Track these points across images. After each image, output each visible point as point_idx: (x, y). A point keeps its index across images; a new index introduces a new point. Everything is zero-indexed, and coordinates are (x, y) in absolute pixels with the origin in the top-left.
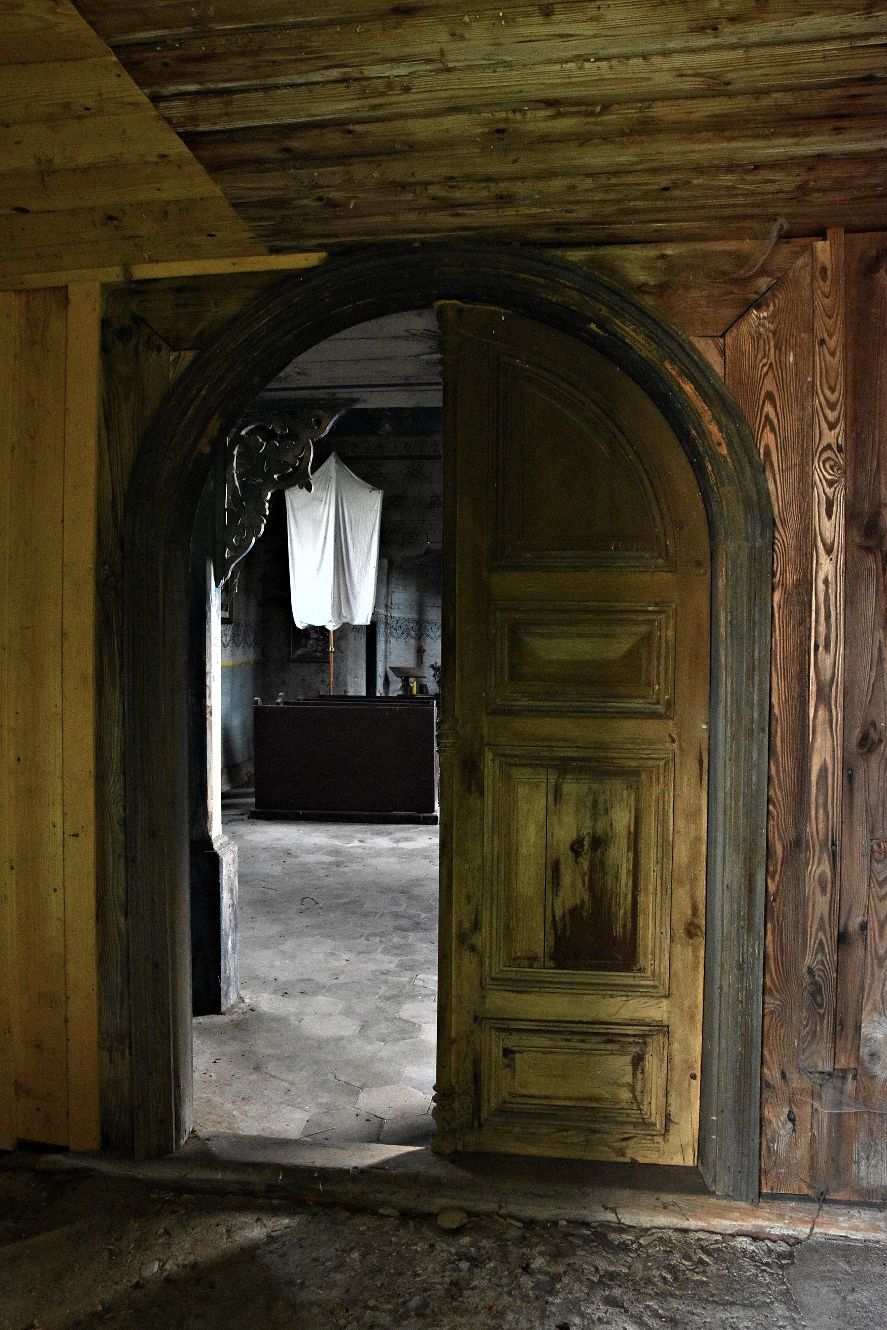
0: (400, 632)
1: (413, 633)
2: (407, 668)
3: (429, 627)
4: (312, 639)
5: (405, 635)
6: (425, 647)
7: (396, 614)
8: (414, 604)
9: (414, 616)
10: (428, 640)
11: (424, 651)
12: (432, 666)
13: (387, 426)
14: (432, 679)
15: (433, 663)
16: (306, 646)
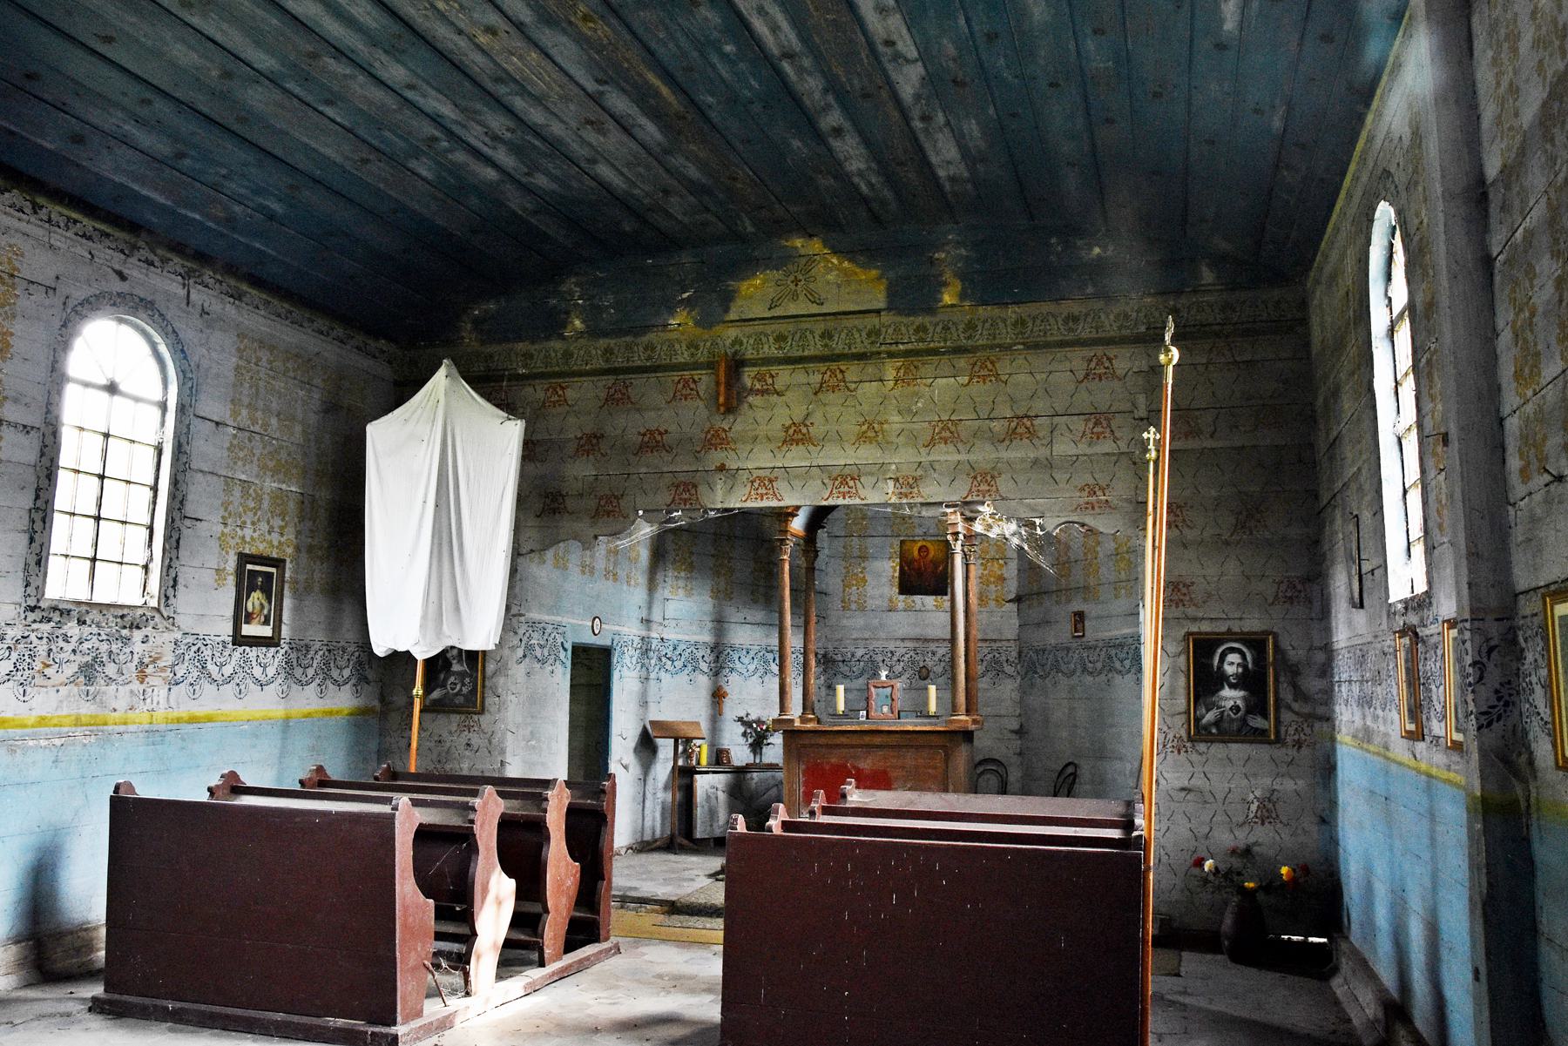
0: (679, 664)
1: (704, 666)
2: (678, 723)
3: (736, 657)
4: (455, 673)
6: (726, 689)
7: (671, 635)
8: (707, 619)
9: (707, 638)
10: (734, 678)
11: (724, 695)
12: (740, 719)
13: (577, 323)
14: (742, 740)
15: (742, 714)
16: (444, 686)
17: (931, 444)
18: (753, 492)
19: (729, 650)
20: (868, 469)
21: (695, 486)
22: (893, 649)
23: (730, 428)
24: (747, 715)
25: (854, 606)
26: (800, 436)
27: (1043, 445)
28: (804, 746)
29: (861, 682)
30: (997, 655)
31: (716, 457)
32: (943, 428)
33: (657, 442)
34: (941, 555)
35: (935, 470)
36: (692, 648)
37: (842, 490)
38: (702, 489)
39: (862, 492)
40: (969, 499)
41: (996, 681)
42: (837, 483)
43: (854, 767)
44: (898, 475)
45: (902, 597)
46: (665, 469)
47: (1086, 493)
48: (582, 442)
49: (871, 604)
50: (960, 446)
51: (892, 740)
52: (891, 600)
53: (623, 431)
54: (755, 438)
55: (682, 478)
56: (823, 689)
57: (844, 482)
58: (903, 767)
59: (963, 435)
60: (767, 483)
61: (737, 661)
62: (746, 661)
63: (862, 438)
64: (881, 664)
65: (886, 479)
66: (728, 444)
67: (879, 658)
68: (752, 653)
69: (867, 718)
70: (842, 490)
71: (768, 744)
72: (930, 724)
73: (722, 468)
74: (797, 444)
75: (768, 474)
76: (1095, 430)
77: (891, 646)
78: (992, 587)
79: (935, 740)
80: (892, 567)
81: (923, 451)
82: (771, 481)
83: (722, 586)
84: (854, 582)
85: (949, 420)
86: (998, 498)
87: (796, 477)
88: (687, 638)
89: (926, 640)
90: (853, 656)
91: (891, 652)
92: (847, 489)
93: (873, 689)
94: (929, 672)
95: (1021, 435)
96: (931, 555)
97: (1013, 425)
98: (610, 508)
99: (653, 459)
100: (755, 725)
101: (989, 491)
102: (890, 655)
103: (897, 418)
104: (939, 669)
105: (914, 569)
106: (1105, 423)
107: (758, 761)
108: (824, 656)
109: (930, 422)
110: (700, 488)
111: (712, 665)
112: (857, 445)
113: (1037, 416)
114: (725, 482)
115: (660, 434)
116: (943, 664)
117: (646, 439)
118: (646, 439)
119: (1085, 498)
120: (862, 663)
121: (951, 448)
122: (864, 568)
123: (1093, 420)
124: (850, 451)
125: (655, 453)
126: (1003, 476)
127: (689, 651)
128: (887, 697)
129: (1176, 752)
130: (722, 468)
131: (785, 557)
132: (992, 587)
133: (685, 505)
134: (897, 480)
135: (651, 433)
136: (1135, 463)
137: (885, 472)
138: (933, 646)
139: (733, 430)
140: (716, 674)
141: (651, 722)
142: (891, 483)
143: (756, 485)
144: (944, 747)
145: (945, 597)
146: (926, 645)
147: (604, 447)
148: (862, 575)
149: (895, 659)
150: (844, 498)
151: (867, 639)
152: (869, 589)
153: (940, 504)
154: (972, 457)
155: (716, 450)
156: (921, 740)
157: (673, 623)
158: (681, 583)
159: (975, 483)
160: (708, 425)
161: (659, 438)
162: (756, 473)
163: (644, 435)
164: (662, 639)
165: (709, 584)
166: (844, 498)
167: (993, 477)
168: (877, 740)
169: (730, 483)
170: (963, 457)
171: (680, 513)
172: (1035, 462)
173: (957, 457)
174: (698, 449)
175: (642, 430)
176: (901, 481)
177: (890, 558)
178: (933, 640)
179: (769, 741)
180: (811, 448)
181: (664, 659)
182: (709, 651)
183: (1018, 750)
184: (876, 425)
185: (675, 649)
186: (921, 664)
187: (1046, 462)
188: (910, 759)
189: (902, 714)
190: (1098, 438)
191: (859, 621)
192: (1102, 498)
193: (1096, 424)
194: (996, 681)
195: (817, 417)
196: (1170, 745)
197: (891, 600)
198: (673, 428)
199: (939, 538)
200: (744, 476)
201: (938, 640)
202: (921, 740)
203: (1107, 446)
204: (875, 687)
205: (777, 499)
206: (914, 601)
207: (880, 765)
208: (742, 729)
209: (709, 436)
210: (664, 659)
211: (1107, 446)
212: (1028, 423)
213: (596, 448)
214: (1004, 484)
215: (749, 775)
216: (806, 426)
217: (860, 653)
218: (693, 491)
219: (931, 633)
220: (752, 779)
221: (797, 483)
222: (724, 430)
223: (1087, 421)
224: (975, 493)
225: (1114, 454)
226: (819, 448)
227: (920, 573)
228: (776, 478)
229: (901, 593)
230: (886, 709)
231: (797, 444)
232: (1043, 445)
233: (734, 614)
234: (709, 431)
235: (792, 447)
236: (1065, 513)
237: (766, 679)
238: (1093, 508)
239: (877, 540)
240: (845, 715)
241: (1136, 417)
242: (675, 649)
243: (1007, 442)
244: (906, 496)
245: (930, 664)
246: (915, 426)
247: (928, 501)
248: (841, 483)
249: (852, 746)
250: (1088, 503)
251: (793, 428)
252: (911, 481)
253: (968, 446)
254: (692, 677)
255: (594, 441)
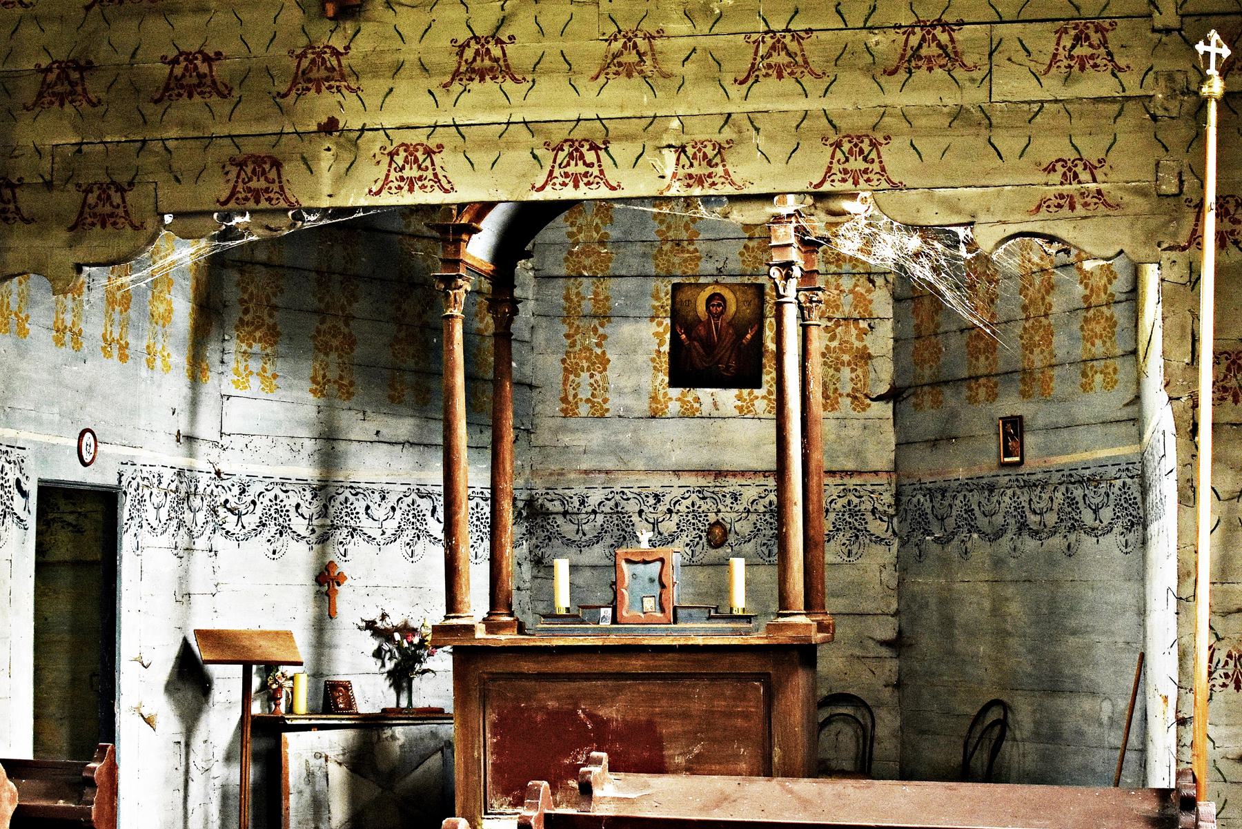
0: (251, 521)
1: (299, 525)
2: (250, 635)
3: (360, 506)
5: (272, 529)
6: (343, 567)
8: (304, 432)
9: (308, 471)
10: (357, 548)
11: (339, 580)
12: (370, 625)
14: (374, 664)
15: (374, 615)
17: (750, 77)
18: (393, 176)
19: (347, 493)
20: (624, 127)
21: (277, 165)
22: (660, 491)
23: (347, 48)
24: (384, 616)
25: (584, 410)
26: (487, 63)
27: (973, 80)
28: (495, 677)
29: (596, 554)
30: (856, 501)
31: (323, 104)
32: (773, 48)
33: (201, 76)
34: (747, 312)
35: (757, 130)
36: (277, 491)
37: (571, 169)
38: (291, 170)
39: (612, 175)
40: (827, 187)
41: (855, 548)
42: (561, 155)
43: (590, 716)
44: (685, 139)
45: (675, 392)
46: (218, 130)
47: (1056, 177)
48: (52, 77)
49: (615, 403)
50: (807, 80)
51: (665, 664)
52: (654, 399)
53: (134, 55)
54: (398, 68)
55: (249, 148)
56: (526, 567)
57: (576, 155)
58: (685, 715)
59: (815, 60)
60: (421, 158)
61: (363, 516)
62: (379, 512)
63: (612, 66)
64: (635, 518)
65: (660, 148)
66: (343, 78)
67: (632, 507)
68: (392, 499)
69: (614, 620)
70: (570, 170)
71: (425, 671)
72: (735, 632)
73: (330, 127)
74: (482, 79)
75: (424, 140)
76: (1077, 51)
77: (655, 483)
78: (846, 373)
79: (752, 665)
80: (656, 334)
81: (735, 91)
82: (429, 153)
83: (333, 374)
84: (585, 365)
85: (787, 30)
86: (884, 185)
87: (484, 144)
88: (262, 470)
89: (719, 474)
90: (582, 503)
91: (656, 496)
92: (581, 169)
93: (624, 565)
94: (726, 533)
95: (929, 59)
96: (732, 308)
97: (914, 41)
98: (108, 209)
99: (191, 108)
100: (397, 636)
101: (866, 171)
102: (652, 501)
103: (685, 27)
104: (744, 527)
105: (700, 340)
106: (1095, 38)
107: (404, 703)
108: (530, 503)
109: (748, 35)
110: (286, 167)
111: (315, 522)
112: (602, 79)
113: (961, 23)
114: (336, 157)
115: (207, 59)
116: (753, 517)
117: (178, 70)
118: (178, 70)
119: (1054, 186)
120: (600, 518)
121: (788, 84)
122: (604, 337)
123: (1073, 33)
124: (589, 90)
125: (197, 98)
126: (895, 142)
127: (271, 495)
128: (652, 580)
129: (1232, 686)
130: (330, 127)
131: (456, 312)
132: (846, 373)
133: (257, 202)
134: (682, 149)
135: (189, 57)
136: (1154, 118)
137: (658, 136)
138: (732, 484)
139: (352, 52)
140: (323, 540)
141: (198, 633)
142: (670, 156)
143: (399, 160)
144: (763, 677)
145: (756, 392)
146: (721, 481)
147: (95, 88)
148: (599, 351)
149: (662, 508)
150: (576, 186)
151: (607, 472)
152: (611, 374)
153: (768, 198)
154: (832, 104)
155: (319, 91)
156: (722, 665)
157: (239, 442)
158: (255, 365)
159: (839, 155)
160: (303, 41)
161: (203, 68)
162: (399, 137)
163: (175, 61)
164: (218, 473)
165: (307, 367)
166: (576, 186)
167: (874, 145)
168: (636, 664)
169: (347, 157)
170: (814, 104)
171: (247, 218)
172: (959, 114)
173: (802, 105)
174: (283, 88)
175: (172, 54)
176: (690, 151)
177: (652, 318)
178: (734, 474)
179: (424, 666)
180: (509, 85)
181: (221, 511)
182: (309, 496)
183: (894, 680)
184: (639, 41)
185: (243, 492)
186: (712, 518)
187: (979, 115)
188: (699, 699)
189: (680, 612)
190: (1082, 68)
191: (595, 437)
192: (1093, 186)
193: (1077, 39)
194: (855, 548)
195: (522, 27)
196: (1221, 672)
197: (654, 399)
198: (231, 47)
199: (746, 280)
200: (374, 144)
201: (743, 473)
202: (722, 665)
203: (1098, 84)
204: (628, 561)
205: (442, 188)
206: (697, 400)
207: (642, 713)
208: (373, 644)
209: (305, 63)
210: (221, 511)
211: (1098, 84)
212: (944, 38)
213: (79, 89)
214: (895, 158)
215: (388, 732)
216: (499, 42)
217: (595, 497)
218: (273, 174)
219: (732, 459)
220: (393, 737)
221: (482, 158)
222: (336, 53)
223: (1062, 32)
224: (839, 176)
225: (1113, 100)
226: (527, 86)
227: (709, 346)
228: (440, 147)
229: (673, 384)
230: (650, 604)
231: (482, 79)
232: (973, 80)
233: (355, 426)
234: (304, 55)
235: (472, 86)
236: (1018, 217)
237: (418, 548)
238: (1072, 207)
239: (628, 285)
240: (570, 617)
241: (1158, 25)
242: (243, 492)
243: (902, 75)
244: (700, 181)
245: (728, 516)
246: (721, 41)
247: (745, 191)
248: (570, 155)
249: (588, 677)
250: (1061, 196)
251: (474, 46)
252: (710, 152)
253: (827, 81)
254: (277, 545)
255: (75, 75)
